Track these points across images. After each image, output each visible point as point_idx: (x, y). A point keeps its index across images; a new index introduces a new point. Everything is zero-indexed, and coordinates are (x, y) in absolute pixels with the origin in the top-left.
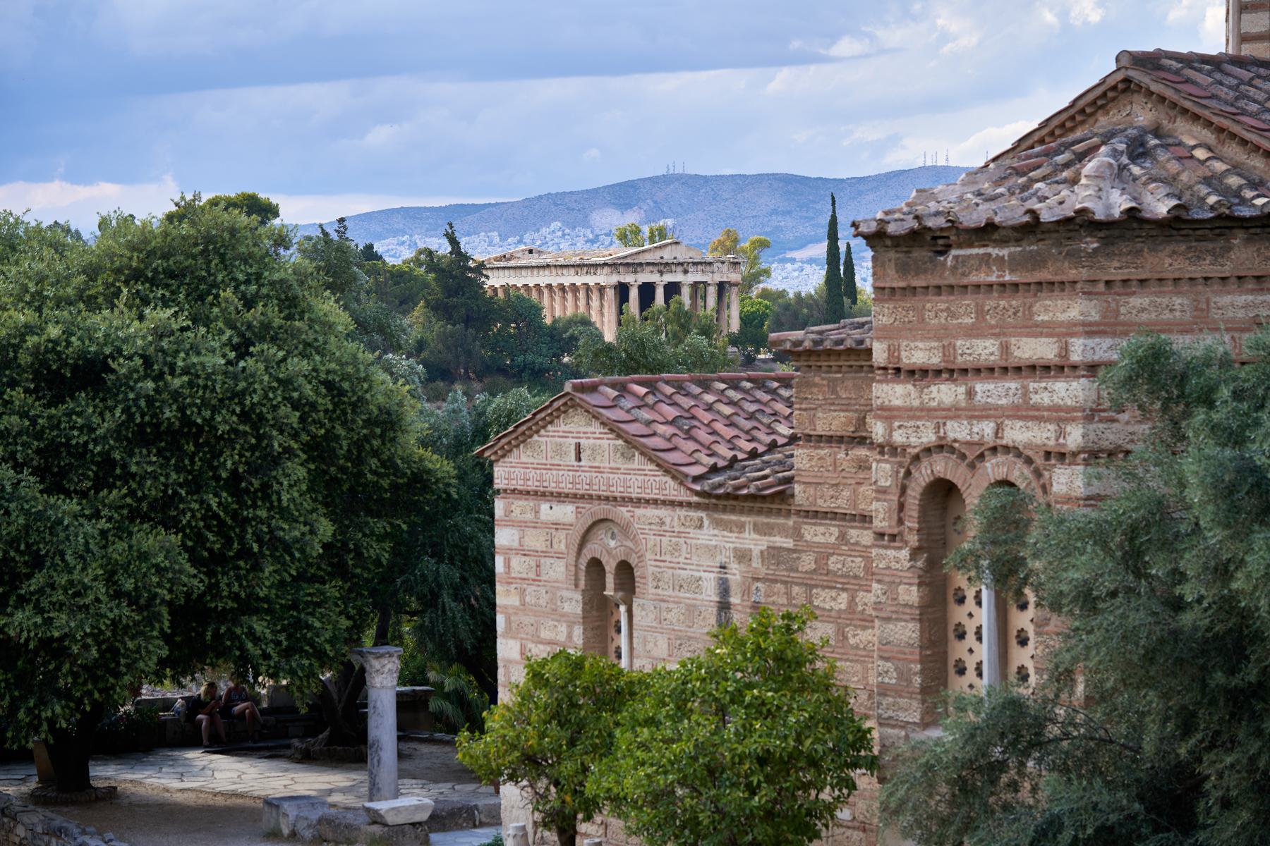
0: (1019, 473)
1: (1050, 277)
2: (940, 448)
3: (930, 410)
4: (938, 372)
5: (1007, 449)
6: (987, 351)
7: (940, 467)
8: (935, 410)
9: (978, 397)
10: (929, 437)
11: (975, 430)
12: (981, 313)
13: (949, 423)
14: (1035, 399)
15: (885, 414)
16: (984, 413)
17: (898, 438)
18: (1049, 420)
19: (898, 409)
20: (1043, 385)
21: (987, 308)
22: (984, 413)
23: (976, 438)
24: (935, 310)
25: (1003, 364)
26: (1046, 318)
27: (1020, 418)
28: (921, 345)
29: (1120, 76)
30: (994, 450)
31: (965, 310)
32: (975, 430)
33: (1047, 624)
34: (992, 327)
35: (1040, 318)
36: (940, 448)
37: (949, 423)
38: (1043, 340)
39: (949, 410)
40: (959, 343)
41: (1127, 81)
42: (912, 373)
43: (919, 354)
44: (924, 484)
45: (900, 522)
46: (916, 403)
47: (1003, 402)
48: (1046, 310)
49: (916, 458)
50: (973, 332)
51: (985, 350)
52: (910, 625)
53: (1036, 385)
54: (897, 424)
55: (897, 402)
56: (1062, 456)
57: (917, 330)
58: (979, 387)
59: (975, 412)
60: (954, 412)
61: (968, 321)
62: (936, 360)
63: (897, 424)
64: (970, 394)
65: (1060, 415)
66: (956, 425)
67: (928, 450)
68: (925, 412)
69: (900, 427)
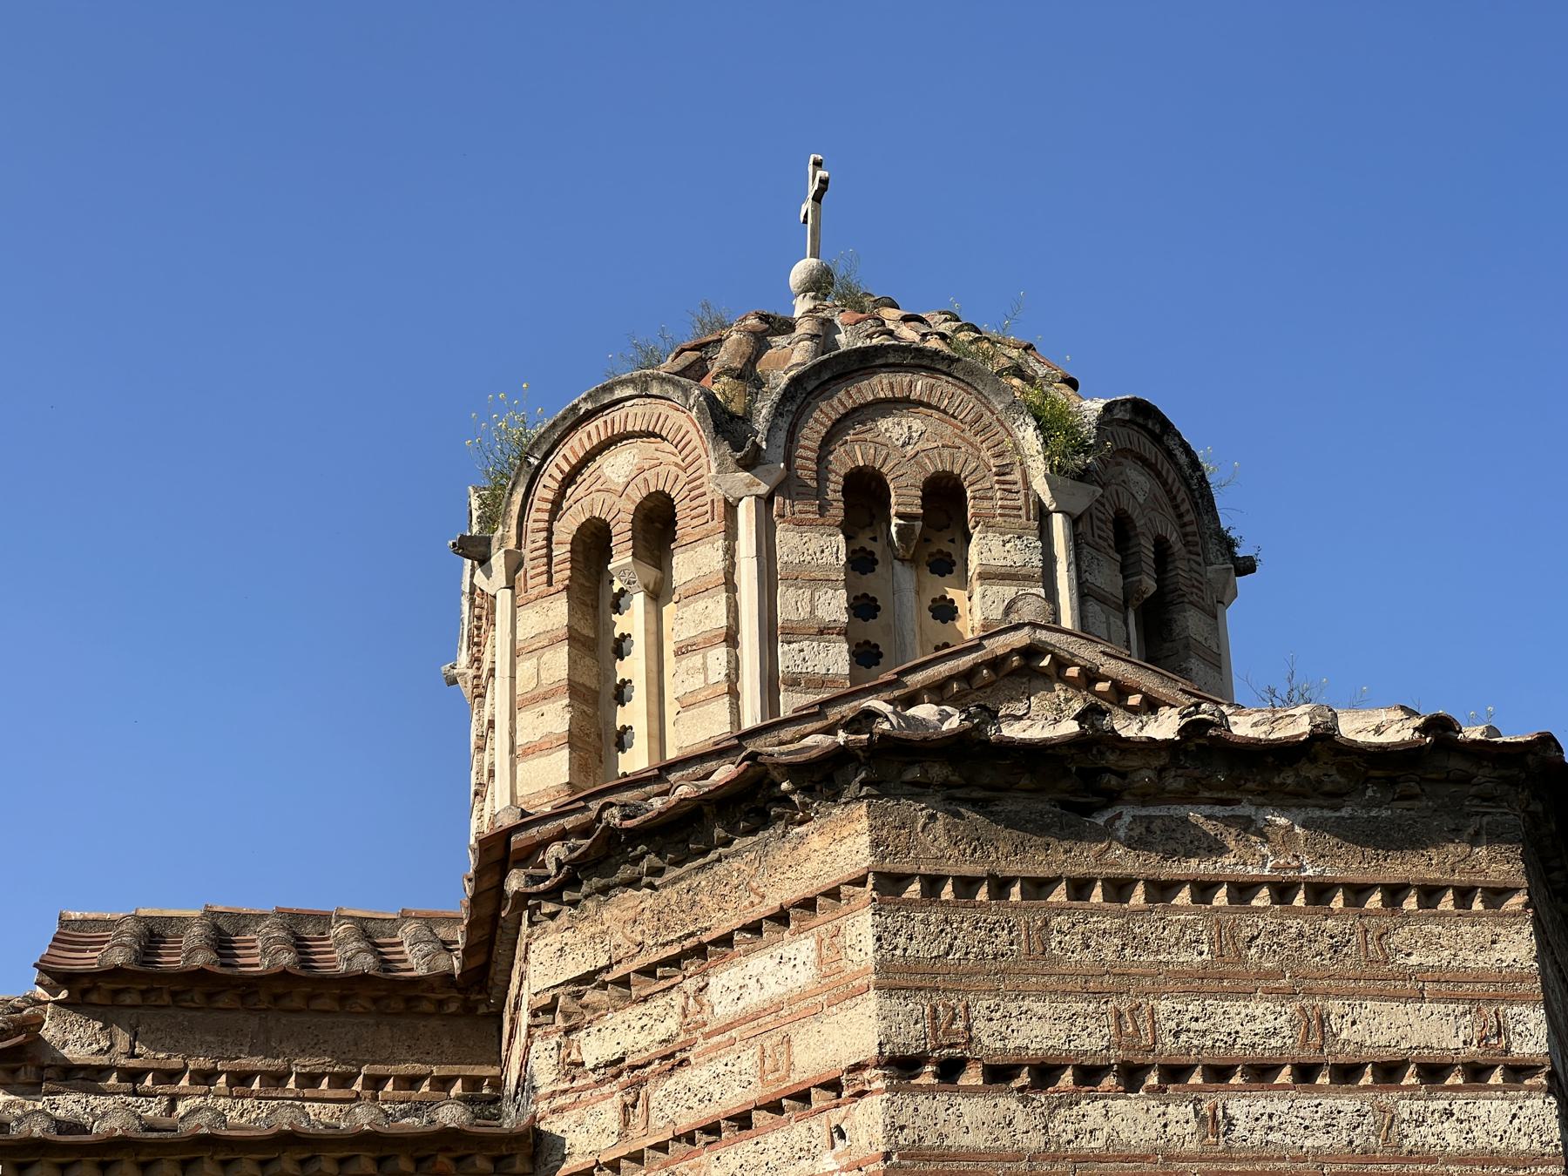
1: (1433, 875)
4: (1089, 1075)
6: (1258, 1027)
8: (1100, 1159)
9: (1240, 1130)
12: (1228, 942)
14: (1414, 1137)
20: (1442, 1104)
21: (1247, 932)
24: (1085, 935)
25: (1309, 1056)
26: (1432, 960)
28: (1038, 1008)
29: (1020, 638)
31: (1182, 936)
34: (1268, 975)
35: (1414, 960)
38: (1427, 1007)
39: (1144, 1158)
40: (1164, 1006)
41: (1031, 652)
42: (999, 1074)
43: (1035, 1029)
46: (1035, 1141)
47: (1322, 1140)
48: (1430, 943)
50: (1199, 983)
51: (1257, 1023)
53: (1418, 1105)
55: (976, 1140)
57: (1033, 972)
58: (1237, 1108)
62: (1093, 1041)
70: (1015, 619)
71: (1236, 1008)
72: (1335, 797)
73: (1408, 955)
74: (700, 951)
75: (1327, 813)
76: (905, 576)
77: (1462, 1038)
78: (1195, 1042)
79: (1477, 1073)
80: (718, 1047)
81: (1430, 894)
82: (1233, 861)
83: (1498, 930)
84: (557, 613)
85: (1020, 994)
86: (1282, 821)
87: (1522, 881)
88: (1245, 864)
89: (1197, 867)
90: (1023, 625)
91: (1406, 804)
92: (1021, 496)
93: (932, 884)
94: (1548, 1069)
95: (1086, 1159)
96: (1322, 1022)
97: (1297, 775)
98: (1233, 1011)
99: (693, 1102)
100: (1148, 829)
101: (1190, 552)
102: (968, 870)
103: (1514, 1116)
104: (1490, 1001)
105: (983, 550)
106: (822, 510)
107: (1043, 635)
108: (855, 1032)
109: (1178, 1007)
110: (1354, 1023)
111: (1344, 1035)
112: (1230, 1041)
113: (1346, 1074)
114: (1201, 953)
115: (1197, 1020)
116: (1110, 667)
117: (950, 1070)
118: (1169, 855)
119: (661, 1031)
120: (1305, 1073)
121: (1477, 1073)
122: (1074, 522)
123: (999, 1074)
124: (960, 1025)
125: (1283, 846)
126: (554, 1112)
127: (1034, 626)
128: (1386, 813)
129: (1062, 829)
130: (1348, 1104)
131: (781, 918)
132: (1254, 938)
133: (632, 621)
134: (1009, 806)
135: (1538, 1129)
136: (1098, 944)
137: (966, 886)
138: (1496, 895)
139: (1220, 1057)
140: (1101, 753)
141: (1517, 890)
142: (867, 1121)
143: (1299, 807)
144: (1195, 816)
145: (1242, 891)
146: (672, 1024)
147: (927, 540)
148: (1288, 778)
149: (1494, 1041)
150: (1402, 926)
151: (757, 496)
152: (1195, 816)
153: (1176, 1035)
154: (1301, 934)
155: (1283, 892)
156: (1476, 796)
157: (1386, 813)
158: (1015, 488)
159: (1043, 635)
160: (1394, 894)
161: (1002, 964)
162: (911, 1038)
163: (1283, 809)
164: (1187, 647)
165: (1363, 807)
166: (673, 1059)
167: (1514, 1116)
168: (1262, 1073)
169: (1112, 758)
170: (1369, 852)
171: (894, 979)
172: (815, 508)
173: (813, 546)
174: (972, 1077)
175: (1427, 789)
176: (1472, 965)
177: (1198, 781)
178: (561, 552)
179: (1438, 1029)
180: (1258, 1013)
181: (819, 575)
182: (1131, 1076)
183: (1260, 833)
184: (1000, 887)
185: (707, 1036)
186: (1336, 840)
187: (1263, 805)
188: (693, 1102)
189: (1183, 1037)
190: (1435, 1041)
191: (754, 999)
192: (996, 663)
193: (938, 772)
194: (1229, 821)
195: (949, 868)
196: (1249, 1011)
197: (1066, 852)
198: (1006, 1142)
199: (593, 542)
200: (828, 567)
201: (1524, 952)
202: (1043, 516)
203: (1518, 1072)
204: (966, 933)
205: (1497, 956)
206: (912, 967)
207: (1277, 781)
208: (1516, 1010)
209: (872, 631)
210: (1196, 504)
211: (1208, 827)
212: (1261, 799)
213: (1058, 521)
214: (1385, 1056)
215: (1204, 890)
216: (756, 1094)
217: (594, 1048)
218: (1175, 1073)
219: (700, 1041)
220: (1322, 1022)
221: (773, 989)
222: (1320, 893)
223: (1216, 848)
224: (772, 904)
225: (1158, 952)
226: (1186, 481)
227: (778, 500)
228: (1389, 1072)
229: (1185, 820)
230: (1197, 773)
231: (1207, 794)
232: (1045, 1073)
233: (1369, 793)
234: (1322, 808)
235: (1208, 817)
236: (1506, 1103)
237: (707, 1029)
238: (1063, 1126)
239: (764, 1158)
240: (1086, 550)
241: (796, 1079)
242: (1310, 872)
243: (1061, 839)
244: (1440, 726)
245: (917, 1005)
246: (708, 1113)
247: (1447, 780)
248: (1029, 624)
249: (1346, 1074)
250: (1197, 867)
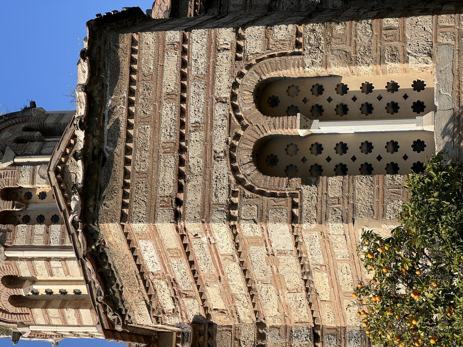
0: (251, 81)
2: (233, 159)
3: (205, 166)
4: (182, 162)
5: (234, 96)
6: (169, 113)
7: (244, 155)
8: (206, 160)
9: (199, 120)
10: (223, 167)
11: (220, 122)
13: (215, 148)
14: (202, 71)
15: (207, 210)
16: (209, 114)
17: (223, 198)
18: (215, 57)
19: (204, 197)
20: (193, 63)
21: (142, 114)
22: (209, 114)
23: (226, 122)
24: (141, 161)
25: (178, 99)
27: (213, 83)
28: (162, 176)
29: (52, 175)
30: (235, 108)
31: (142, 133)
32: (220, 122)
33: (349, 53)
34: (155, 109)
35: (152, 67)
36: (233, 159)
37: (215, 148)
39: (206, 147)
40: (163, 139)
41: (57, 172)
42: (181, 188)
43: (168, 177)
44: (256, 172)
45: (283, 196)
46: (200, 179)
47: (202, 96)
48: (147, 62)
49: (240, 182)
50: (156, 129)
51: (168, 113)
52: (357, 185)
53: (193, 69)
54: (214, 199)
55: (199, 196)
56: (239, 49)
57: (151, 177)
58: (192, 120)
59: (208, 124)
60: (208, 142)
61: (149, 131)
62: (172, 160)
63: (214, 199)
64: (197, 126)
65: (214, 49)
66: (217, 141)
67: (235, 170)
68: (207, 166)
69: (216, 196)
70: (46, 176)
71: (164, 119)
72: (103, 86)
73: (150, 68)
74: (142, 274)
75: (108, 89)
76: (32, 207)
77: (174, 55)
78: (173, 131)
79: (184, 52)
80: (170, 270)
81: (133, 61)
82: (121, 117)
83: (144, 42)
84: (38, 312)
85: (158, 181)
86: (110, 102)
87: (130, 34)
88: (122, 114)
89: (123, 127)
90: (48, 173)
91: (106, 66)
92: (8, 171)
93: (124, 205)
94: (184, 32)
95: (206, 165)
96: (169, 94)
97: (97, 97)
98: (165, 120)
99: (186, 277)
100: (111, 141)
101: (28, 121)
102: (121, 195)
103: (197, 42)
104: (164, 46)
105: (25, 183)
106: (10, 231)
107: (52, 168)
108: (167, 230)
109: (163, 135)
110: (169, 85)
111: (173, 88)
112: (173, 121)
113: (184, 88)
114: (148, 128)
115: (167, 130)
116: (62, 148)
117: (179, 203)
118: (119, 135)
119: (165, 286)
120: (183, 100)
121: (184, 52)
122: (17, 155)
123: (181, 188)
124: (166, 199)
125: (117, 102)
126: (187, 318)
127: (48, 170)
128: (109, 72)
129: (110, 166)
130: (192, 89)
131: (133, 250)
132: (144, 112)
133: (41, 289)
134: (102, 182)
135: (201, 35)
136: (144, 157)
137: (125, 195)
138: (134, 42)
139: (178, 124)
140: (88, 154)
141: (132, 36)
142: (192, 227)
143: (106, 97)
144: (108, 127)
145: (130, 115)
146: (163, 283)
147: (21, 200)
148: (97, 99)
149: (176, 46)
150: (142, 70)
151: (4, 250)
152: (108, 127)
153: (171, 136)
154: (143, 99)
155: (131, 103)
156: (105, 46)
157: (109, 72)
158: (6, 173)
159: (52, 168)
160: (132, 71)
161: (148, 186)
162: (169, 214)
163: (106, 101)
164: (57, 124)
165: (107, 78)
166: (173, 283)
167: (197, 42)
168: (183, 112)
169: (90, 151)
170: (120, 77)
171: (152, 218)
172: (9, 233)
173: (21, 234)
174: (181, 196)
175: (102, 59)
176: (154, 51)
177: (97, 126)
178: (19, 310)
179: (172, 62)
180: (165, 112)
181: (30, 232)
182: (182, 150)
183: (113, 108)
184: (126, 185)
185: (167, 273)
186: (116, 87)
187: (105, 107)
188: (186, 277)
189: (172, 134)
190: (175, 63)
191: (156, 259)
192: (59, 182)
193: (91, 202)
194: (110, 117)
195: (120, 200)
196: (165, 115)
197: (117, 166)
198: (200, 187)
199: (16, 300)
200: (28, 230)
201: (150, 35)
202: (15, 164)
203: (185, 40)
204: (139, 196)
205: (151, 43)
206: (148, 212)
207: (98, 103)
208: (167, 39)
209: (48, 217)
210: (13, 118)
211: (111, 123)
212: (103, 108)
213: (16, 160)
214: (179, 77)
215: (129, 126)
216: (184, 260)
217: (169, 306)
218: (182, 137)
219: (168, 275)
220: (169, 94)
221: (154, 253)
222: (131, 92)
223: (117, 122)
224: (128, 252)
225: (147, 140)
226: (6, 121)
227: (6, 244)
228: (183, 76)
229: (109, 130)
230: (95, 126)
231: (101, 123)
232: (181, 175)
233: (103, 76)
234: (106, 90)
235: (108, 123)
236: (193, 44)
237: (165, 273)
238: (196, 171)
239: (202, 257)
240: (26, 152)
241: (180, 247)
242: (125, 95)
243: (113, 167)
244: (84, 54)
245: (160, 211)
246: (189, 273)
247: (100, 53)
248: (48, 172)
249: (184, 88)
250: (123, 127)
